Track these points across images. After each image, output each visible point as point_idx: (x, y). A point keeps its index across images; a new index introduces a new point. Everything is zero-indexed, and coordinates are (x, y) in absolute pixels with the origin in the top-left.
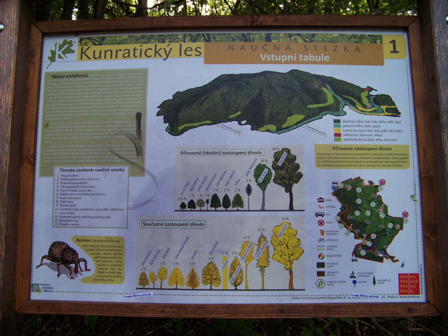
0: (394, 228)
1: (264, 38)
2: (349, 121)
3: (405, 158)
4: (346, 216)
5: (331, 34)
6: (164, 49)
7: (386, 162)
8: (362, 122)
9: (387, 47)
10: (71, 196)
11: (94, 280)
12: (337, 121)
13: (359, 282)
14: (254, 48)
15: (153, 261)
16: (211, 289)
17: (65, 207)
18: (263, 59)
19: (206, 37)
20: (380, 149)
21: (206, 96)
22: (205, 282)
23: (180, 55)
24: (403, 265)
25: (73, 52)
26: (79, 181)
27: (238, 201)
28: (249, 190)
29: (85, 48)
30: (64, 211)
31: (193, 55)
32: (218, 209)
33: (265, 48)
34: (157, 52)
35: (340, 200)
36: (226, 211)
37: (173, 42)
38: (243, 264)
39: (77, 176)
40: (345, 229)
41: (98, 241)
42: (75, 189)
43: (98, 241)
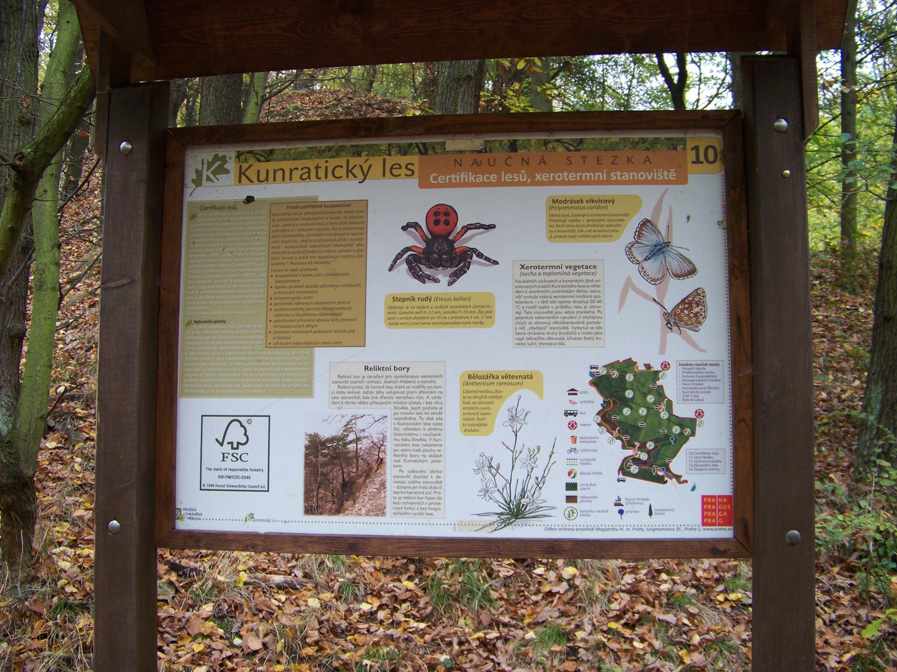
0: (681, 434)
4: (609, 415)
6: (361, 166)
13: (627, 512)
19: (422, 148)
23: (384, 175)
25: (228, 172)
29: (245, 166)
34: (349, 171)
35: (601, 393)
37: (373, 155)
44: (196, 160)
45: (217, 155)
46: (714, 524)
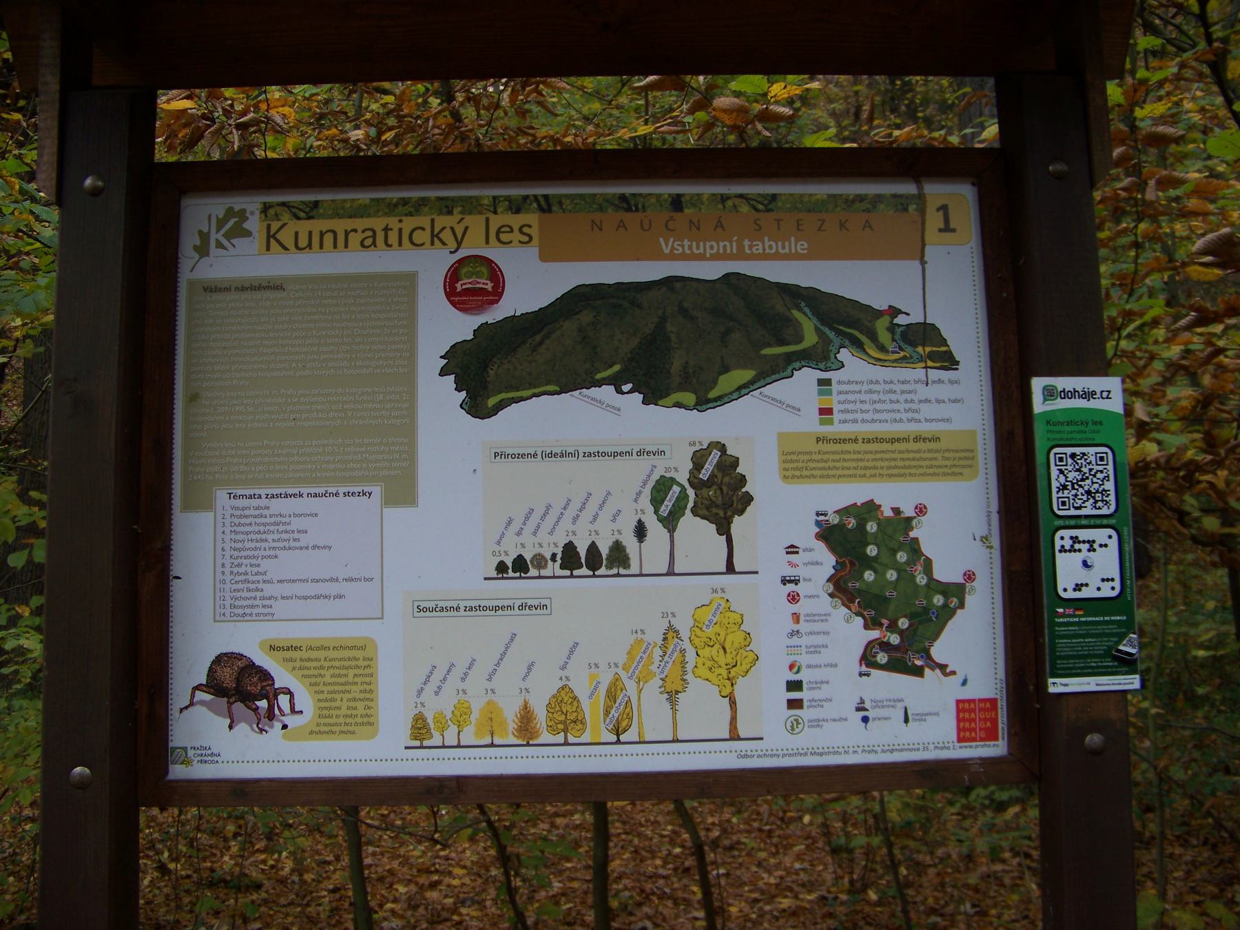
0: (945, 606)
2: (849, 382)
4: (845, 583)
6: (452, 229)
8: (877, 382)
10: (256, 553)
11: (311, 733)
13: (874, 719)
14: (646, 227)
15: (439, 688)
16: (566, 744)
17: (242, 578)
18: (667, 251)
19: (543, 203)
21: (544, 332)
22: (552, 729)
23: (487, 242)
24: (964, 683)
25: (248, 234)
26: (273, 520)
27: (619, 556)
28: (641, 531)
29: (275, 226)
30: (240, 586)
31: (516, 243)
32: (576, 572)
35: (832, 549)
36: (594, 576)
37: (470, 213)
38: (631, 688)
39: (268, 508)
40: (844, 610)
41: (318, 649)
42: (263, 537)
43: (318, 649)
44: (201, 213)
46: (974, 740)
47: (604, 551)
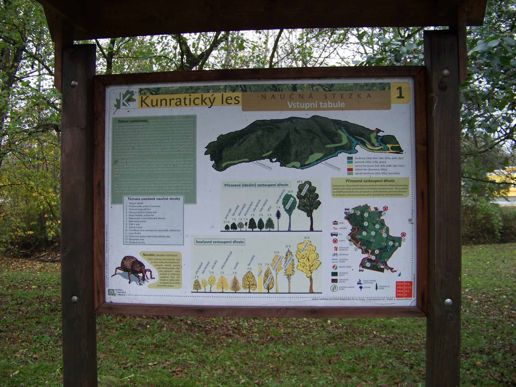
0: (393, 246)
1: (290, 88)
2: (360, 158)
3: (405, 189)
5: (347, 84)
6: (209, 98)
7: (389, 192)
8: (371, 158)
9: (395, 93)
10: (138, 220)
11: (158, 286)
12: (350, 158)
14: (282, 97)
15: (204, 271)
16: (249, 293)
17: (133, 229)
18: (290, 107)
20: (385, 181)
21: (244, 138)
22: (244, 287)
23: (222, 103)
24: (400, 275)
25: (135, 100)
26: (144, 208)
27: (270, 224)
28: (278, 215)
30: (132, 232)
31: (233, 104)
32: (254, 230)
33: (292, 96)
34: (203, 101)
35: (351, 223)
36: (261, 231)
38: (274, 273)
39: (142, 203)
40: (354, 246)
41: (160, 255)
42: (141, 214)
43: (160, 255)
45: (128, 91)
47: (265, 222)
